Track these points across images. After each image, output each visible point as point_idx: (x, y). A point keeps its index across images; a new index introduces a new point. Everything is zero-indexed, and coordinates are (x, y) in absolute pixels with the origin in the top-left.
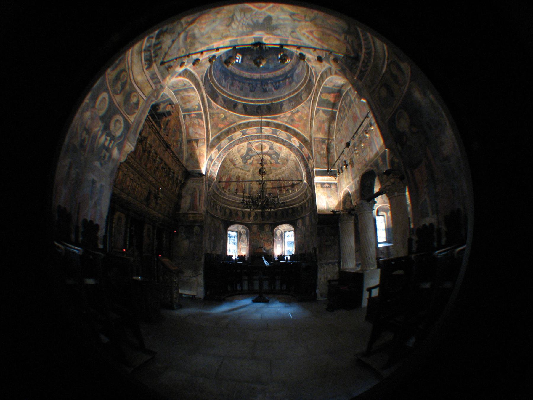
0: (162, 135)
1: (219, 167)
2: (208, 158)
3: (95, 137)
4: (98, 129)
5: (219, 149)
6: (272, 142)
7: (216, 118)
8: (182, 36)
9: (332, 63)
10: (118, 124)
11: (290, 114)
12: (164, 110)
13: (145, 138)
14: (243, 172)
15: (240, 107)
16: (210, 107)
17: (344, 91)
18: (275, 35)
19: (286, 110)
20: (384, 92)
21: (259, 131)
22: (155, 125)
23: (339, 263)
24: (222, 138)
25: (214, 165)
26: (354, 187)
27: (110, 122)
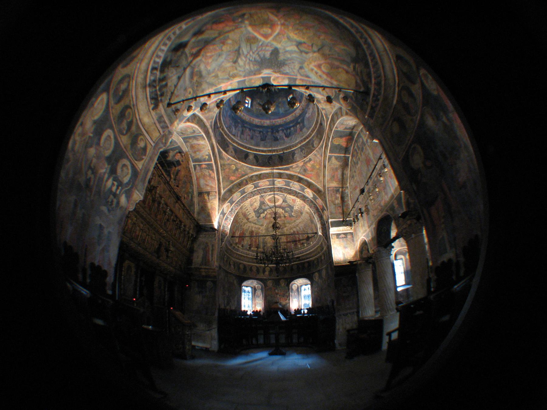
0: (172, 185)
1: (232, 221)
2: (220, 212)
3: (101, 180)
4: (104, 171)
5: (232, 202)
6: (286, 195)
7: (227, 170)
8: (188, 71)
9: (342, 101)
10: (125, 169)
11: (302, 164)
12: (174, 159)
13: (155, 188)
14: (257, 226)
15: (251, 157)
16: (221, 158)
17: (355, 133)
18: (283, 74)
19: (298, 159)
20: (396, 128)
21: (272, 183)
22: (165, 174)
23: (358, 312)
24: (234, 191)
25: (226, 219)
26: (370, 235)
27: (117, 165)
